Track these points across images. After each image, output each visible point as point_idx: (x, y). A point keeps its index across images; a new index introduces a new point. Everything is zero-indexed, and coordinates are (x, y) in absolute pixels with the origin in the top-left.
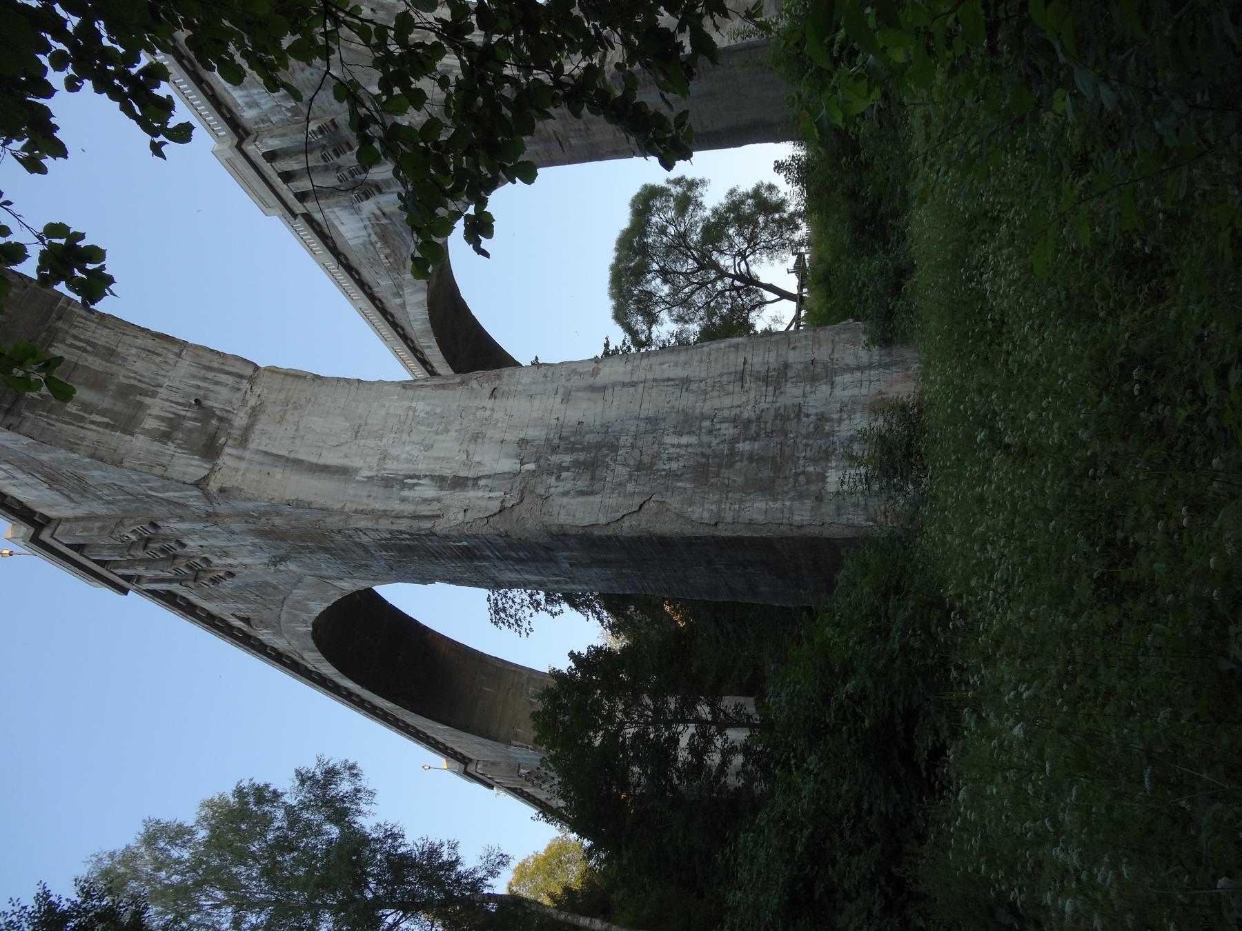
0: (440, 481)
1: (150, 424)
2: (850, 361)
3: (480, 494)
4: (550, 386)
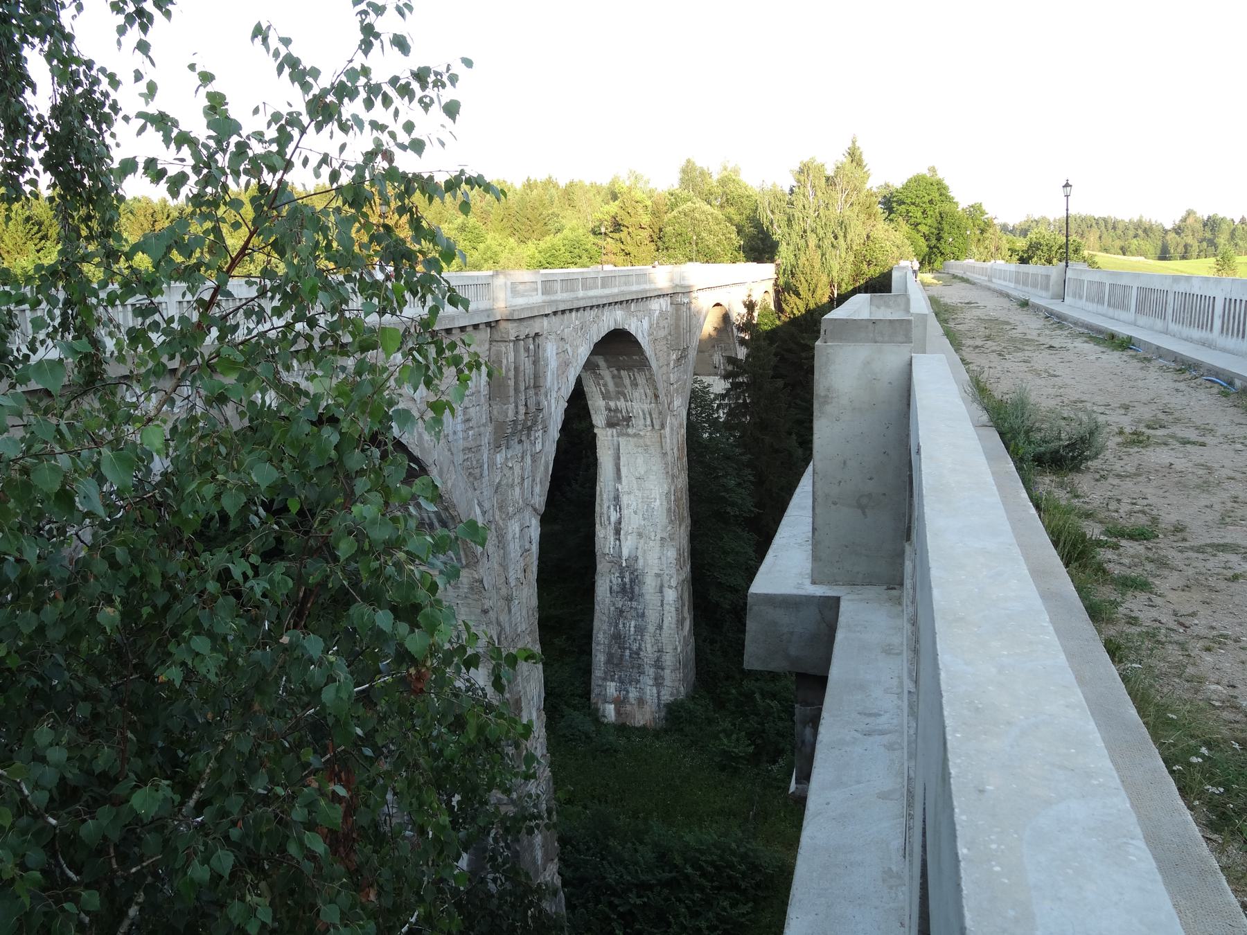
2: (663, 693)
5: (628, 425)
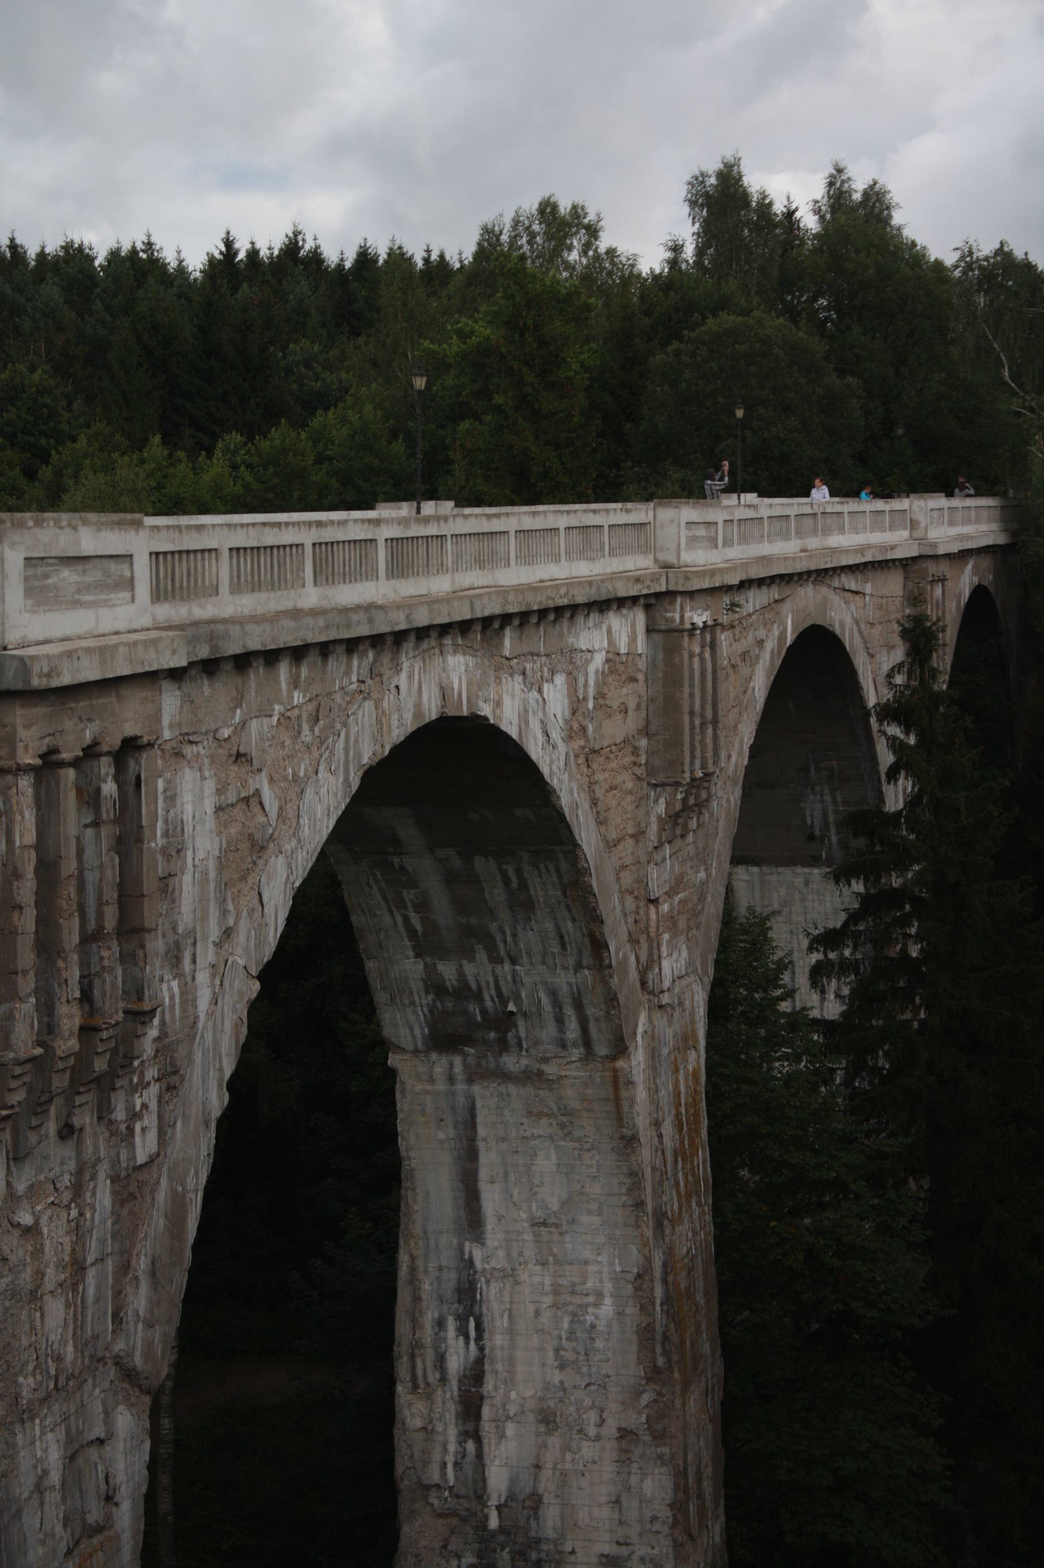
0: (476, 1374)
1: (447, 970)
3: (452, 1448)
4: (633, 1532)
5: (503, 1045)
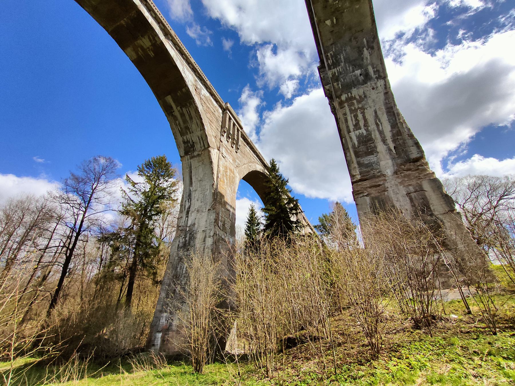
0: (189, 208)
